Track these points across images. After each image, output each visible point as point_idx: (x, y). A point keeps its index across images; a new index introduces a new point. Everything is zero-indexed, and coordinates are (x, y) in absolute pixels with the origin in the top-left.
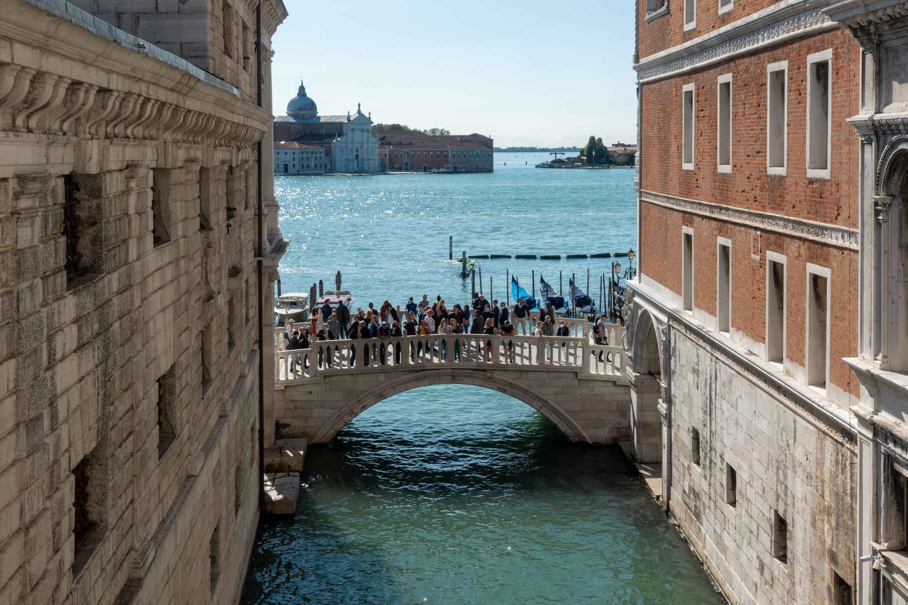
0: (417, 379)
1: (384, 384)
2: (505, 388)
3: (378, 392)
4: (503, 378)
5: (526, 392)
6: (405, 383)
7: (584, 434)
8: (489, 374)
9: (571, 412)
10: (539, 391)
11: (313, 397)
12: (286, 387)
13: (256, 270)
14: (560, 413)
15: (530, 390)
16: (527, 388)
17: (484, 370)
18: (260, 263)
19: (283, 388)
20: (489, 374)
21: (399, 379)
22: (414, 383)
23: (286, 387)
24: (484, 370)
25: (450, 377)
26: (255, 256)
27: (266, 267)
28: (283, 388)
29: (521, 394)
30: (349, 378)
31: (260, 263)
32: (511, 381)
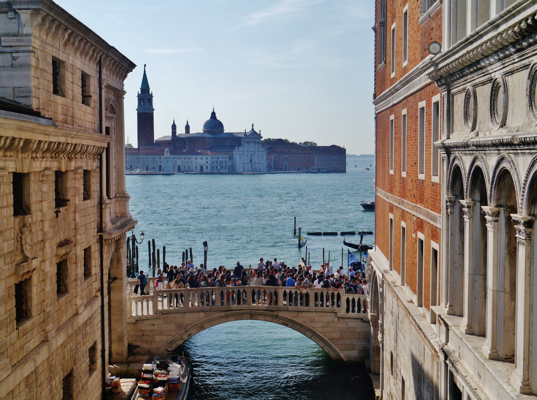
0: (227, 317)
1: (204, 320)
2: (287, 323)
3: (200, 325)
4: (285, 316)
5: (301, 325)
6: (218, 319)
7: (342, 355)
8: (275, 314)
9: (332, 339)
10: (309, 325)
11: (156, 328)
12: (136, 321)
13: (99, 241)
14: (325, 340)
15: (304, 324)
16: (302, 323)
17: (272, 311)
18: (101, 237)
19: (134, 321)
20: (275, 314)
21: (213, 316)
22: (223, 319)
23: (136, 321)
24: (272, 311)
25: (249, 316)
26: (98, 232)
27: (105, 240)
28: (134, 321)
29: (298, 327)
30: (179, 315)
31: (101, 237)
32: (291, 318)
